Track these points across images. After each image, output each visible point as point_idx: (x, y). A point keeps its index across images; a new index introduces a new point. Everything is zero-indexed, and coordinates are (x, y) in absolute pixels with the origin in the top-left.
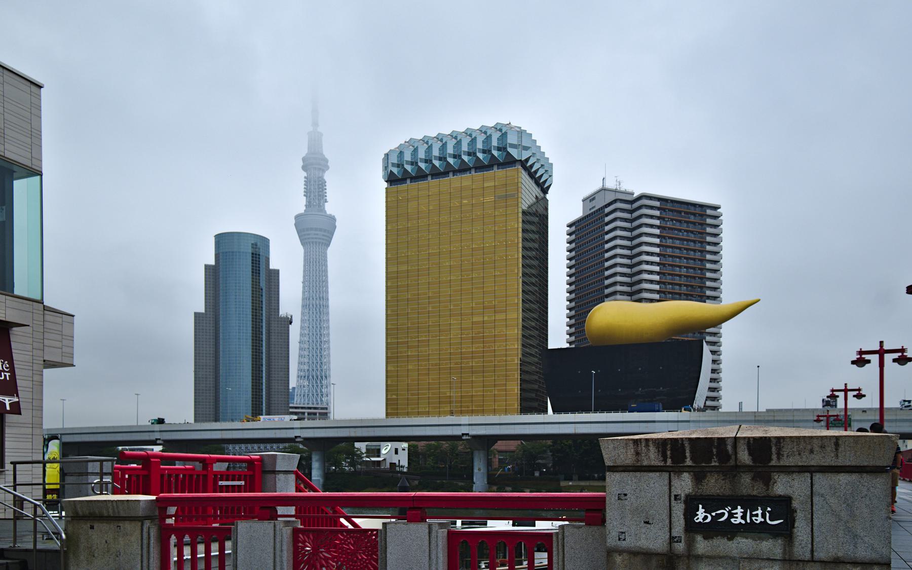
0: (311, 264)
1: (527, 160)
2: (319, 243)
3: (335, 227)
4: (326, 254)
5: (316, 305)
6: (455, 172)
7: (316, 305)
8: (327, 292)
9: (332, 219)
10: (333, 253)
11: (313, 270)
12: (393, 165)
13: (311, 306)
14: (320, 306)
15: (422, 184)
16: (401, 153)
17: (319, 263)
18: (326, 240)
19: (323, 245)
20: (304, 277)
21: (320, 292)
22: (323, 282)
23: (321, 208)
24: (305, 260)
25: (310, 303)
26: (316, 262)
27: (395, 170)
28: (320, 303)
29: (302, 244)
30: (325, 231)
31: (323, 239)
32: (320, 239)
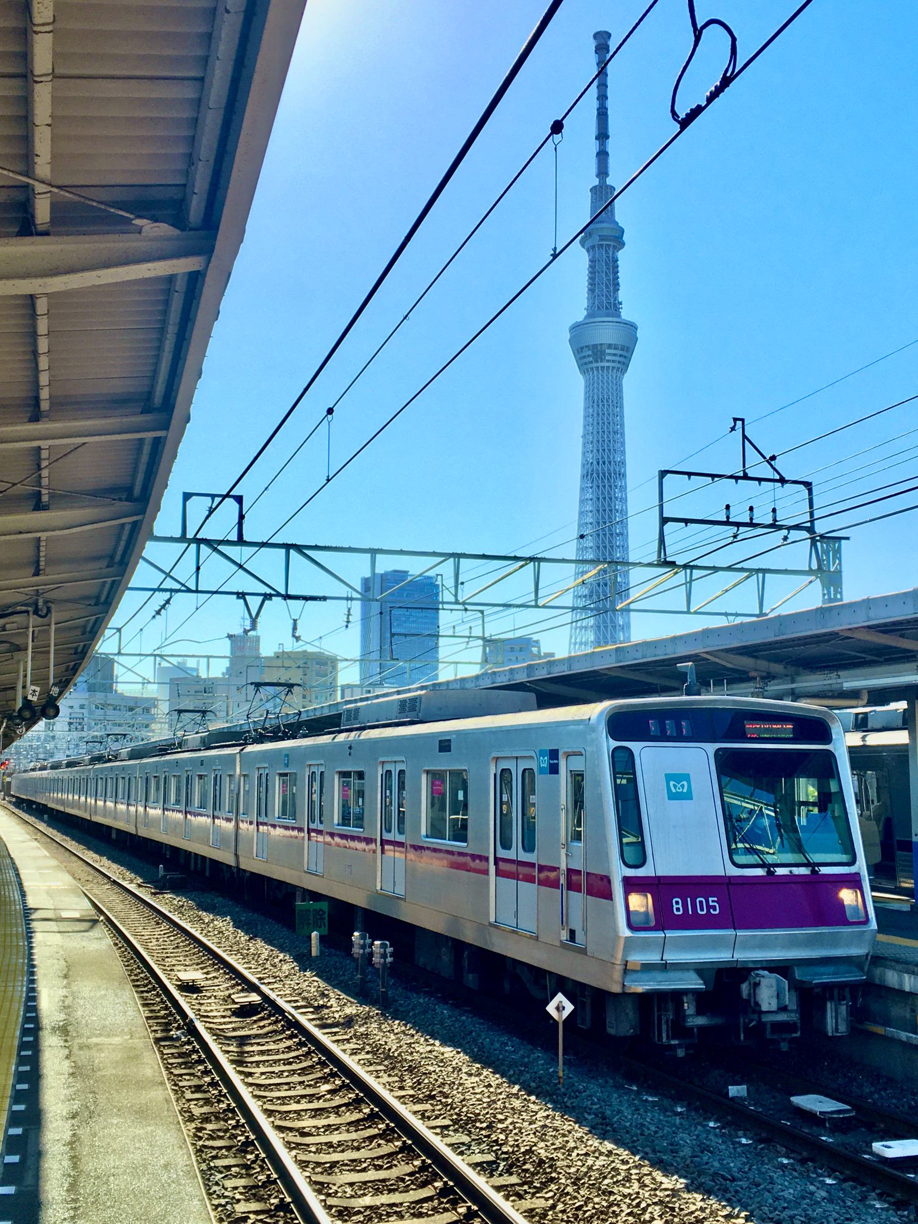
0: (595, 406)
2: (608, 367)
3: (637, 339)
5: (604, 474)
7: (604, 474)
10: (631, 382)
11: (598, 414)
13: (595, 474)
14: (610, 474)
17: (607, 401)
18: (619, 362)
19: (615, 371)
21: (609, 450)
22: (615, 433)
23: (614, 307)
25: (593, 471)
26: (602, 401)
28: (609, 470)
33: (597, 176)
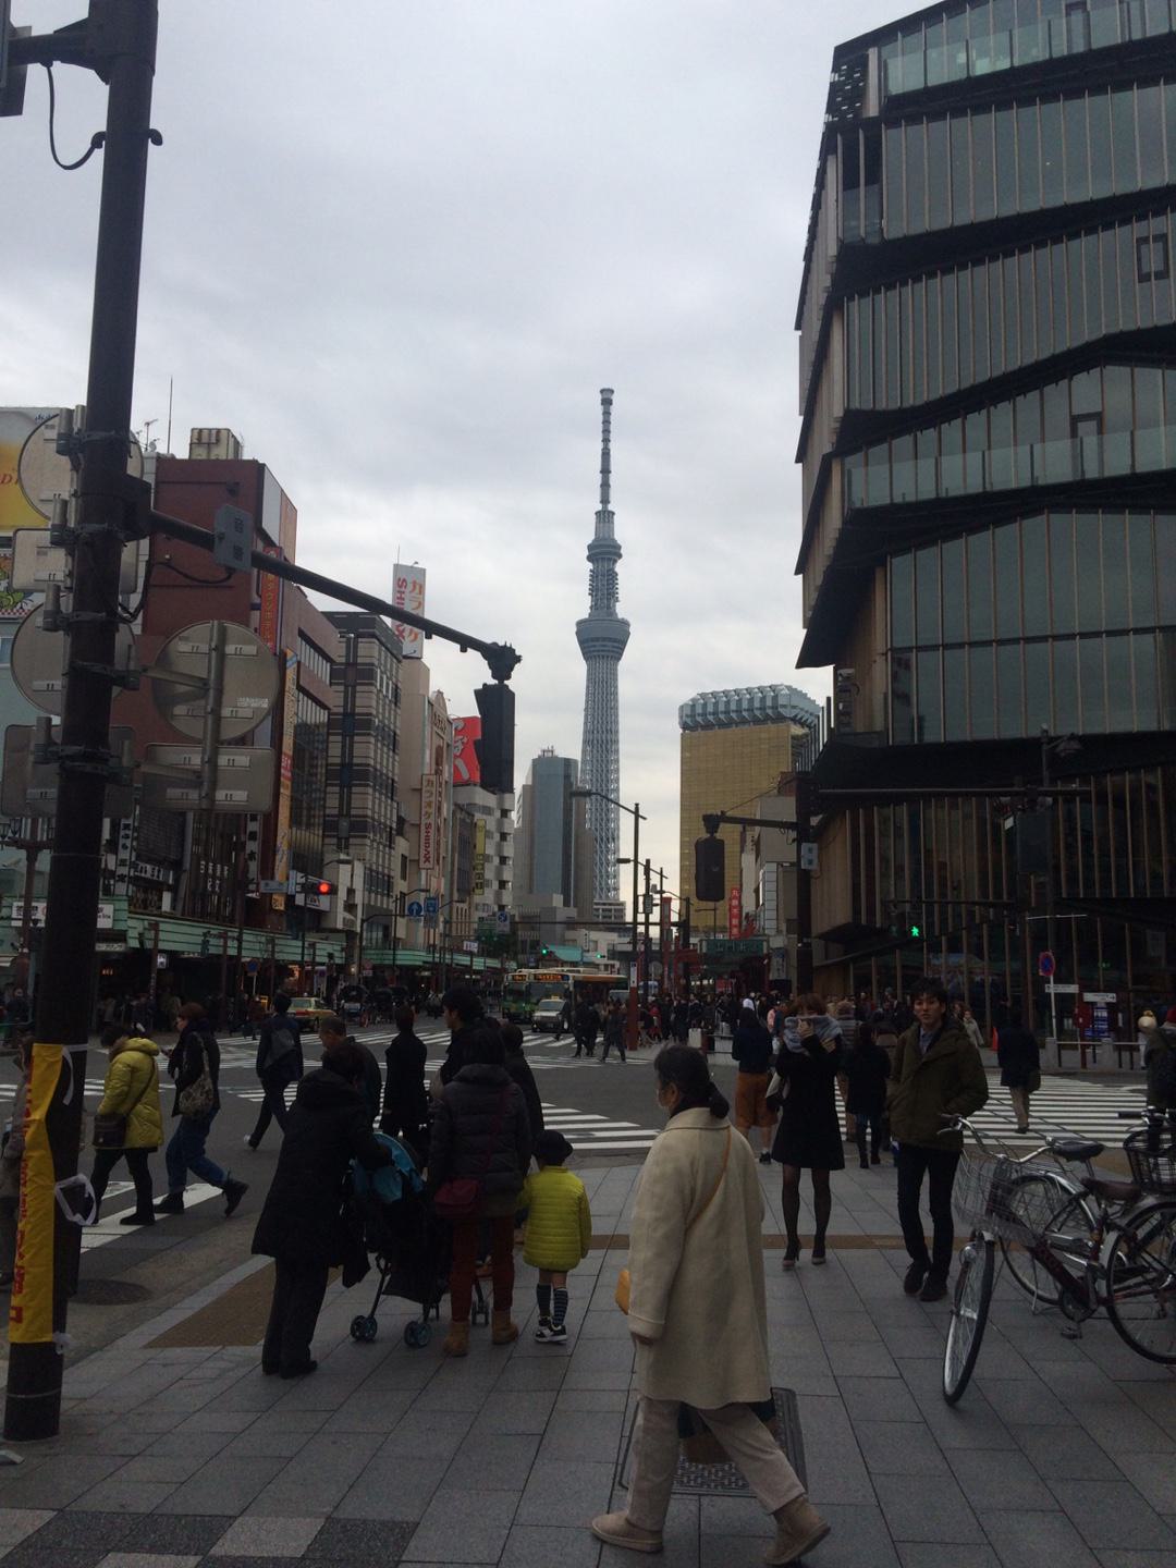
1: (796, 716)
4: (616, 670)
6: (737, 724)
8: (617, 723)
9: (625, 624)
10: (624, 665)
12: (687, 716)
15: (710, 733)
16: (693, 706)
20: (587, 702)
24: (588, 680)
27: (689, 720)
29: (585, 658)
30: (615, 641)
31: (613, 651)
32: (609, 651)
33: (602, 502)
